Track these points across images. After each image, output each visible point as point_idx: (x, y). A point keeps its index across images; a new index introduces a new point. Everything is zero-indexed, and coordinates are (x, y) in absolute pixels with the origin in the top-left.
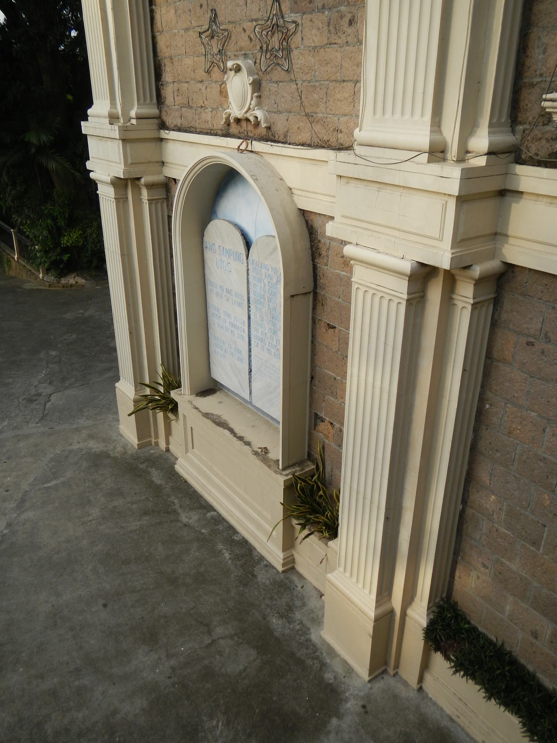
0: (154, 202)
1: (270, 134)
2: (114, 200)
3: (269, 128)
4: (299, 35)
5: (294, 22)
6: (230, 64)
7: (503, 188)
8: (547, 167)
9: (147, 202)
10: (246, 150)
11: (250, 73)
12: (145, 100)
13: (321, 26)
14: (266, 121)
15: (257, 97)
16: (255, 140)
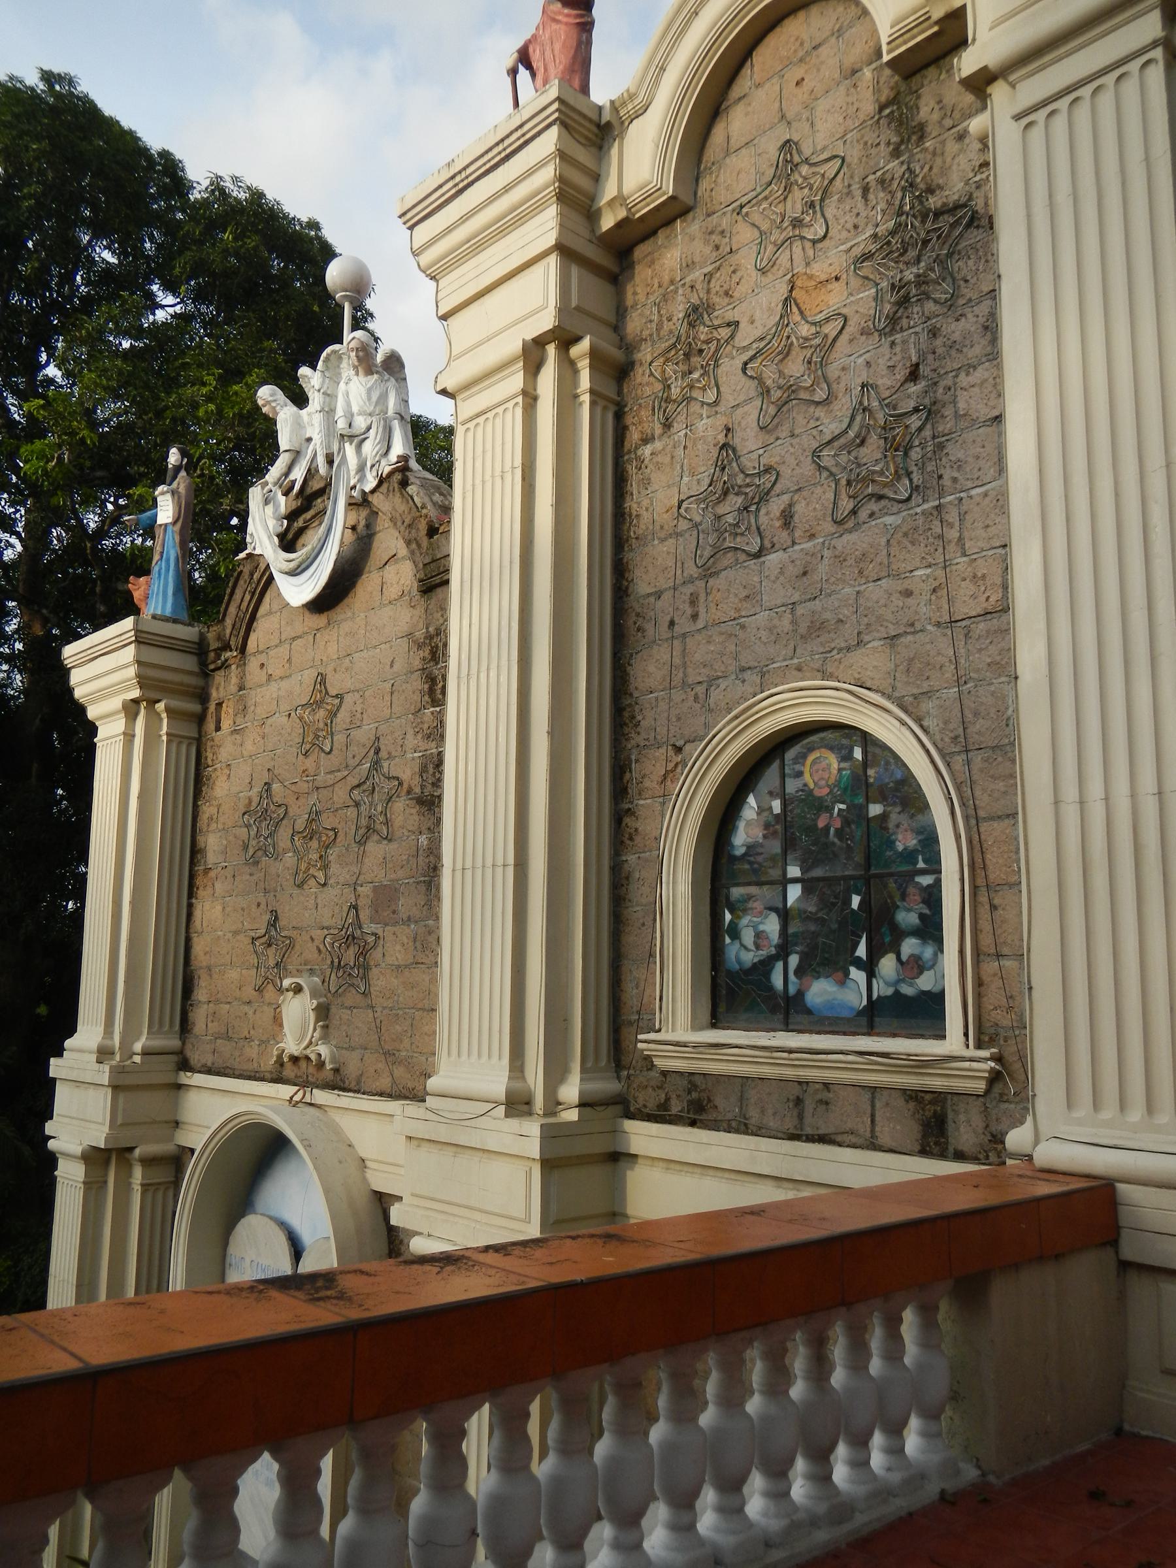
0: (152, 1189)
1: (339, 1078)
2: (82, 1186)
3: (336, 1071)
4: (380, 949)
5: (373, 934)
6: (286, 983)
7: (612, 1150)
8: (657, 1122)
9: (139, 1188)
10: (300, 1101)
11: (314, 994)
12: (161, 1025)
13: (406, 941)
14: (333, 1059)
15: (323, 1027)
16: (317, 1087)
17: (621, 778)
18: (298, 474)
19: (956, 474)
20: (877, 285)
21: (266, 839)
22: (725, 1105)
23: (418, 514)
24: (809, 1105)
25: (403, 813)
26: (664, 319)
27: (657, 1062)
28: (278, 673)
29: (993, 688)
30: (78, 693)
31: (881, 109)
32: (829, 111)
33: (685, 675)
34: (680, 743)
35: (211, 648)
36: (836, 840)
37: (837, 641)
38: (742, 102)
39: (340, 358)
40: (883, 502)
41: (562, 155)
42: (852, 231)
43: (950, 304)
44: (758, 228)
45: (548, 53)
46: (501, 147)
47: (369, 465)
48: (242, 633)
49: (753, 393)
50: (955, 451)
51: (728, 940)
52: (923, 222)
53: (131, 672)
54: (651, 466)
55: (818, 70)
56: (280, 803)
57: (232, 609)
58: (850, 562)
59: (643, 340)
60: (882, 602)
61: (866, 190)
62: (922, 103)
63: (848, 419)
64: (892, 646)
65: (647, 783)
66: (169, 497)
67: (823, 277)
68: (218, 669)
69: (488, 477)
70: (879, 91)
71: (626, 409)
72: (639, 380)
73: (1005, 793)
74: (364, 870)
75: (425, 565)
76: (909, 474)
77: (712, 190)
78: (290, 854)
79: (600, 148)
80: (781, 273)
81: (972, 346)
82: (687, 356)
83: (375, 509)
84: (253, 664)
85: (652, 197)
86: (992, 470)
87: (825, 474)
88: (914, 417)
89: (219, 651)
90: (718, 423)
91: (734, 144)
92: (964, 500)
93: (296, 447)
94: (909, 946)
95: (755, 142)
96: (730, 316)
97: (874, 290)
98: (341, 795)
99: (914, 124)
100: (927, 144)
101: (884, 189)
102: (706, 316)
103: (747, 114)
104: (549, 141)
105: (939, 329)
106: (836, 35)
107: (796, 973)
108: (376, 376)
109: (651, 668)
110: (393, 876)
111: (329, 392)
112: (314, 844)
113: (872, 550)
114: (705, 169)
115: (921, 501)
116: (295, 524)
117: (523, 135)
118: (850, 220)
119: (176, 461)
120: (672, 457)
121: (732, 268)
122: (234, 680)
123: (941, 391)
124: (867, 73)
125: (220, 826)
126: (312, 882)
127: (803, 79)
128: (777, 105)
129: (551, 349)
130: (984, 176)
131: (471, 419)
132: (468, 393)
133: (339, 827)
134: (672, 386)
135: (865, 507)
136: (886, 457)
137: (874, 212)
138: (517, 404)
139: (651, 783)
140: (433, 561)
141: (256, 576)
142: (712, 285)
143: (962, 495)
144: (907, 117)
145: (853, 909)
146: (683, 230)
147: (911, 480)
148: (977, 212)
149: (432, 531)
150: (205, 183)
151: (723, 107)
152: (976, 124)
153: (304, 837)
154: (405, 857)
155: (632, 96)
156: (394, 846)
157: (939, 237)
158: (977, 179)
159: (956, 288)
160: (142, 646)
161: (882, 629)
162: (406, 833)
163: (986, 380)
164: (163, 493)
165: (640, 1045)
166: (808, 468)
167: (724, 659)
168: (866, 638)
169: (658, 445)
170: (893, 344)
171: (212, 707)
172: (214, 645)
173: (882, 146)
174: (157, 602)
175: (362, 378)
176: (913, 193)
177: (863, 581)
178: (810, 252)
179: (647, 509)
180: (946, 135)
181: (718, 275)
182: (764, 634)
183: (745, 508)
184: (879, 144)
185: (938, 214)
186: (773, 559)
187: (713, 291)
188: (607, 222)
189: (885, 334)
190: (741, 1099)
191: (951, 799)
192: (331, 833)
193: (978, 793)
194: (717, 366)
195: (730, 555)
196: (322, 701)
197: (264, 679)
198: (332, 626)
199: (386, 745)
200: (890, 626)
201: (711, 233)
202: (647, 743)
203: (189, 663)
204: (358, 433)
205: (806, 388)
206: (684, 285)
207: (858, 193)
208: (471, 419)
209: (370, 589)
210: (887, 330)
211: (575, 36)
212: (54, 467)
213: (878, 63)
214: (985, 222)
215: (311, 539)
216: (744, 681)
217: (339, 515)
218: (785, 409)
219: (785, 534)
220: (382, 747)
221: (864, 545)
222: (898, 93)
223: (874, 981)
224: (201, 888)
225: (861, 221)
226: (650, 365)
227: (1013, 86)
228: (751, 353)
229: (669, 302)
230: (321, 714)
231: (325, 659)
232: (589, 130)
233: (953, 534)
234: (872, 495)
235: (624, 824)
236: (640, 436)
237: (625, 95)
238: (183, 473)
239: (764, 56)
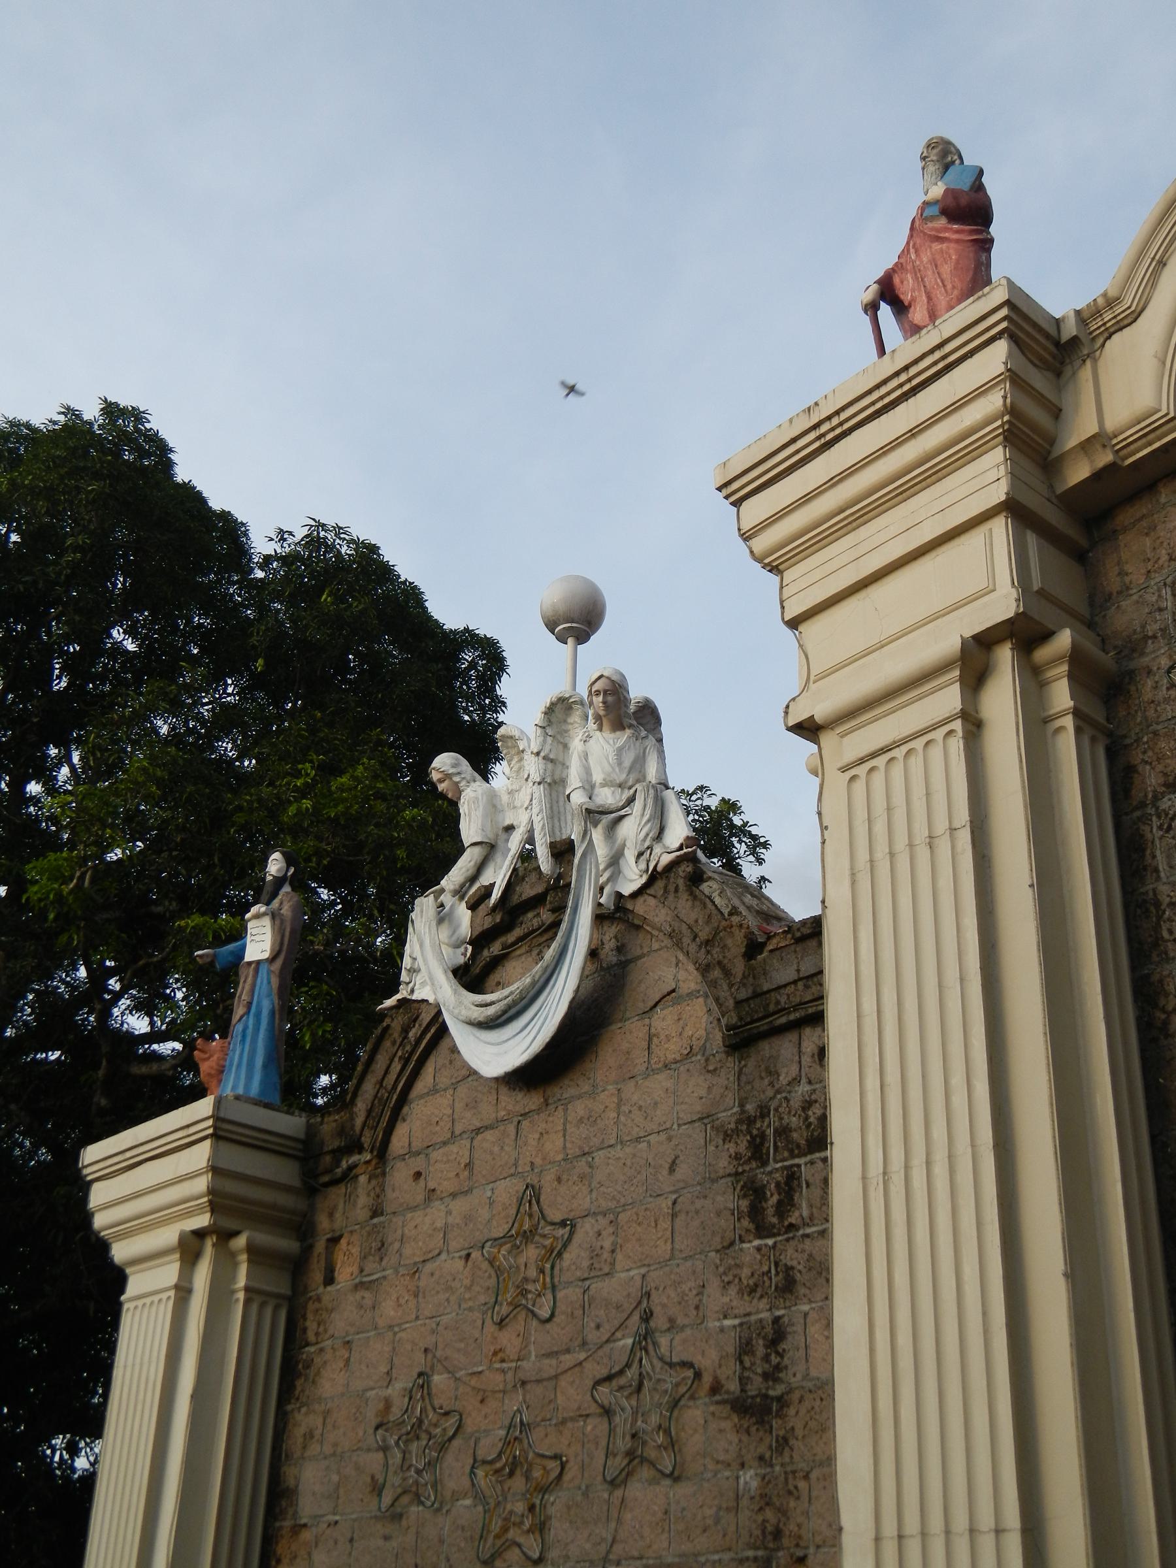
18: (497, 876)
21: (419, 1472)
23: (724, 923)
28: (448, 1186)
30: (99, 1221)
35: (326, 1149)
41: (1013, 377)
46: (903, 377)
47: (630, 855)
48: (383, 1124)
53: (201, 1184)
56: (446, 1408)
59: (1146, 638)
66: (267, 921)
68: (336, 1182)
71: (1128, 741)
72: (1147, 694)
78: (468, 1502)
79: (1058, 374)
83: (636, 922)
84: (399, 1175)
85: (1159, 432)
93: (489, 837)
108: (628, 732)
110: (686, 1547)
111: (552, 756)
112: (518, 1483)
116: (486, 953)
119: (279, 870)
122: (363, 1200)
125: (328, 1449)
126: (514, 1555)
129: (1005, 655)
131: (862, 761)
132: (853, 723)
138: (951, 732)
140: (756, 995)
141: (412, 1034)
150: (300, 533)
153: (497, 1471)
154: (709, 1512)
155: (1111, 302)
156: (683, 1490)
160: (221, 1143)
162: (711, 1466)
164: (258, 916)
171: (320, 1246)
172: (334, 1143)
174: (237, 1077)
175: (607, 734)
188: (1078, 472)
192: (554, 1465)
196: (533, 1231)
197: (420, 1198)
198: (552, 1107)
199: (664, 1306)
203: (285, 1172)
204: (613, 807)
209: (625, 1046)
211: (971, 255)
212: (72, 890)
220: (657, 1310)
224: (286, 1561)
226: (1169, 672)
230: (531, 1253)
231: (538, 1161)
232: (1045, 349)
236: (1161, 780)
238: (287, 889)
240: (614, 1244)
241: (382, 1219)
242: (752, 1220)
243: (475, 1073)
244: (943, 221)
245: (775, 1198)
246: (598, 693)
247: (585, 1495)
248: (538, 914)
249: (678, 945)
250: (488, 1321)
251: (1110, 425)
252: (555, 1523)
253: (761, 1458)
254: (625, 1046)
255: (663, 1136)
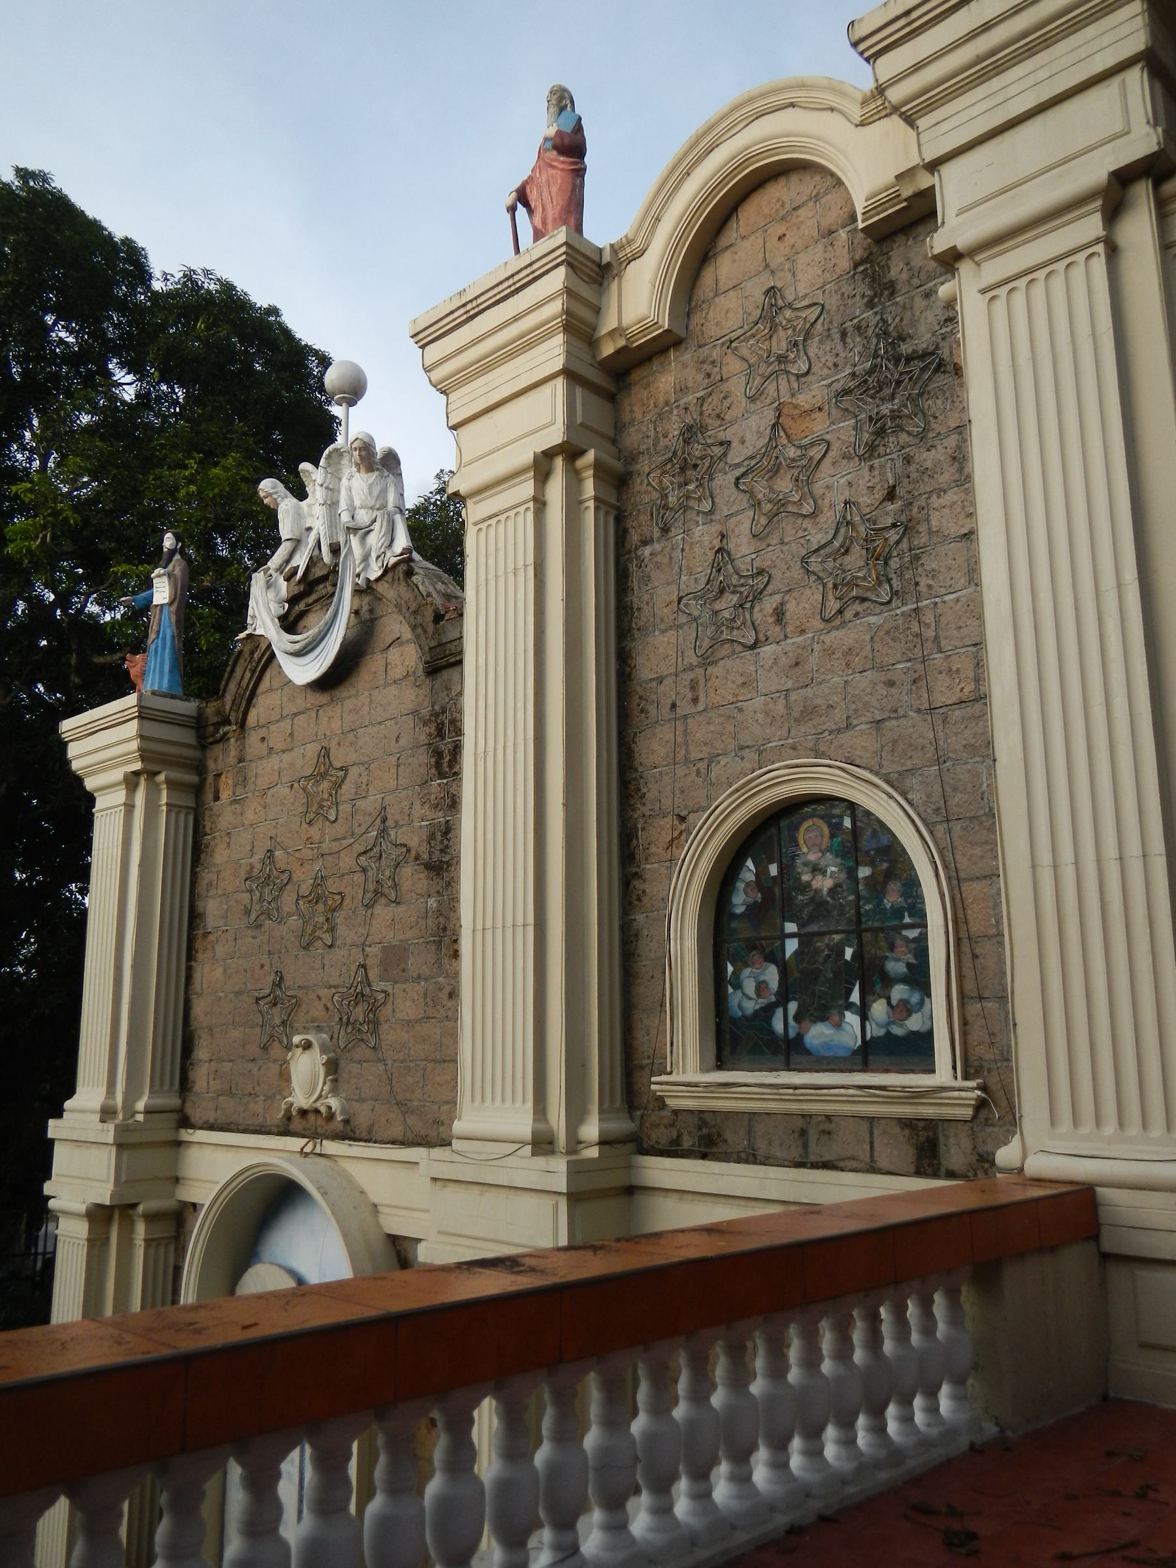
1: (349, 1129)
2: (86, 1243)
3: (346, 1122)
4: (389, 1006)
5: (383, 991)
6: (296, 1039)
7: (627, 1183)
8: (670, 1157)
9: (142, 1243)
10: (312, 1153)
11: (324, 1050)
12: (162, 1085)
13: (416, 997)
14: (344, 1111)
15: (332, 1081)
16: (327, 1138)
17: (629, 845)
18: (301, 561)
19: (931, 582)
20: (857, 416)
21: (269, 903)
22: (734, 1138)
23: (423, 602)
24: (813, 1136)
25: (412, 879)
26: (660, 435)
27: (668, 1102)
28: (280, 746)
29: (969, 767)
30: (75, 765)
31: (856, 266)
32: (809, 264)
33: (687, 752)
34: (683, 814)
36: (829, 899)
37: (828, 724)
38: (729, 251)
39: (341, 455)
40: (866, 604)
41: (569, 292)
42: (833, 368)
43: (922, 436)
44: (747, 361)
45: (545, 193)
46: (511, 282)
47: (374, 556)
49: (745, 505)
50: (929, 563)
51: (730, 990)
52: (896, 365)
53: (134, 745)
54: (650, 565)
55: (799, 228)
56: (283, 869)
57: (232, 686)
58: (838, 655)
60: (868, 690)
61: (844, 335)
62: (892, 264)
63: (833, 532)
64: (878, 729)
65: (653, 849)
66: (165, 579)
67: (807, 407)
68: (218, 742)
69: (501, 572)
70: (854, 250)
71: (626, 514)
72: (637, 488)
73: (982, 857)
74: (372, 931)
75: (431, 649)
76: (889, 580)
77: (702, 325)
78: (295, 918)
79: (601, 284)
80: (768, 401)
81: (942, 473)
82: (683, 470)
84: (253, 739)
86: (963, 581)
87: (813, 578)
88: (893, 531)
89: (217, 725)
90: (713, 530)
91: (723, 286)
92: (939, 605)
94: (899, 992)
95: (742, 286)
96: (722, 436)
97: (853, 421)
98: (347, 861)
99: (885, 281)
100: (898, 299)
101: (860, 335)
102: (699, 435)
103: (734, 261)
104: (558, 278)
105: (912, 457)
106: (814, 199)
107: (796, 1018)
108: (376, 473)
109: (655, 746)
110: (402, 937)
112: (320, 907)
113: (857, 646)
114: (696, 306)
115: (900, 604)
116: (297, 608)
117: (533, 272)
118: (831, 360)
120: (671, 558)
121: (723, 395)
122: (233, 753)
123: (915, 510)
124: (843, 234)
125: (220, 892)
126: (319, 943)
127: (784, 235)
128: (761, 255)
129: (559, 462)
130: (948, 329)
131: (484, 520)
133: (347, 891)
134: (670, 495)
135: (850, 608)
136: (868, 564)
137: (852, 354)
138: (528, 509)
139: (657, 850)
140: (440, 645)
141: (256, 656)
142: (704, 408)
143: (937, 600)
144: (879, 275)
145: (846, 961)
146: (676, 358)
147: (891, 586)
148: (943, 359)
149: (438, 618)
150: (179, 275)
151: (711, 253)
152: (944, 291)
153: (309, 901)
154: (413, 919)
155: (630, 242)
156: (401, 909)
157: (910, 379)
158: (943, 331)
159: (927, 423)
160: (145, 722)
161: (868, 714)
162: (414, 897)
163: (955, 503)
164: (159, 576)
165: (653, 1087)
166: (797, 572)
167: (724, 738)
168: (855, 722)
169: (657, 547)
170: (872, 468)
171: (210, 779)
172: (214, 719)
173: (858, 297)
174: (153, 679)
175: (364, 475)
176: (887, 340)
177: (850, 672)
178: (795, 385)
179: (648, 604)
180: (913, 293)
181: (710, 399)
182: (760, 716)
183: (741, 605)
184: (854, 296)
185: (909, 359)
186: (767, 650)
187: (706, 413)
188: (608, 349)
189: (864, 459)
190: (749, 1132)
191: (935, 862)
193: (958, 857)
194: (711, 479)
195: (726, 646)
196: (326, 773)
197: (265, 752)
199: (393, 815)
200: (876, 711)
201: (703, 362)
202: (652, 813)
204: (363, 526)
205: (795, 503)
206: (678, 407)
207: (837, 337)
208: (484, 520)
209: (373, 669)
210: (866, 455)
211: (570, 180)
213: (852, 227)
214: (950, 368)
215: (314, 624)
216: (743, 758)
217: (346, 600)
218: (775, 519)
219: (778, 629)
221: (851, 641)
222: (871, 254)
223: (867, 1024)
224: (200, 951)
225: (840, 360)
226: (648, 475)
227: (978, 264)
228: (742, 470)
229: (665, 421)
230: (325, 785)
231: (328, 733)
232: (591, 269)
233: (930, 633)
234: (856, 598)
235: (632, 886)
236: (640, 538)
237: (624, 240)
238: (177, 557)
239: (750, 213)
240: (368, 780)
241: (244, 764)
242: (437, 770)
243: (290, 681)
244: (555, 153)
245: (448, 757)
246: (356, 449)
247: (354, 912)
248: (326, 587)
249: (400, 611)
250: (303, 822)
251: (625, 323)
252: (339, 927)
253: (438, 892)
254: (373, 669)
255: (393, 722)
